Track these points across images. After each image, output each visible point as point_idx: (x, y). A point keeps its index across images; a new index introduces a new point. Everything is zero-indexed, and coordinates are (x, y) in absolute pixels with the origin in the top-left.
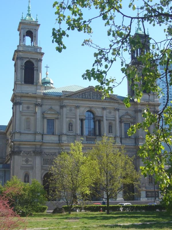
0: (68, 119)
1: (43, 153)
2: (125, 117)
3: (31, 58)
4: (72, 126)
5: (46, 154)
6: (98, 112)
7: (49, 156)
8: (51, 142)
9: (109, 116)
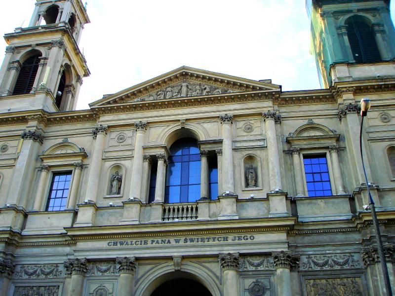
0: (108, 164)
1: (18, 268)
2: (306, 134)
3: (37, 45)
4: (120, 180)
5: (26, 273)
6: (204, 132)
7: (34, 277)
8: (45, 233)
9: (245, 138)
